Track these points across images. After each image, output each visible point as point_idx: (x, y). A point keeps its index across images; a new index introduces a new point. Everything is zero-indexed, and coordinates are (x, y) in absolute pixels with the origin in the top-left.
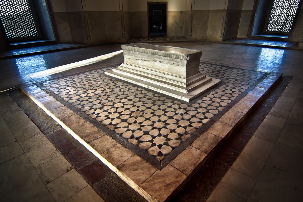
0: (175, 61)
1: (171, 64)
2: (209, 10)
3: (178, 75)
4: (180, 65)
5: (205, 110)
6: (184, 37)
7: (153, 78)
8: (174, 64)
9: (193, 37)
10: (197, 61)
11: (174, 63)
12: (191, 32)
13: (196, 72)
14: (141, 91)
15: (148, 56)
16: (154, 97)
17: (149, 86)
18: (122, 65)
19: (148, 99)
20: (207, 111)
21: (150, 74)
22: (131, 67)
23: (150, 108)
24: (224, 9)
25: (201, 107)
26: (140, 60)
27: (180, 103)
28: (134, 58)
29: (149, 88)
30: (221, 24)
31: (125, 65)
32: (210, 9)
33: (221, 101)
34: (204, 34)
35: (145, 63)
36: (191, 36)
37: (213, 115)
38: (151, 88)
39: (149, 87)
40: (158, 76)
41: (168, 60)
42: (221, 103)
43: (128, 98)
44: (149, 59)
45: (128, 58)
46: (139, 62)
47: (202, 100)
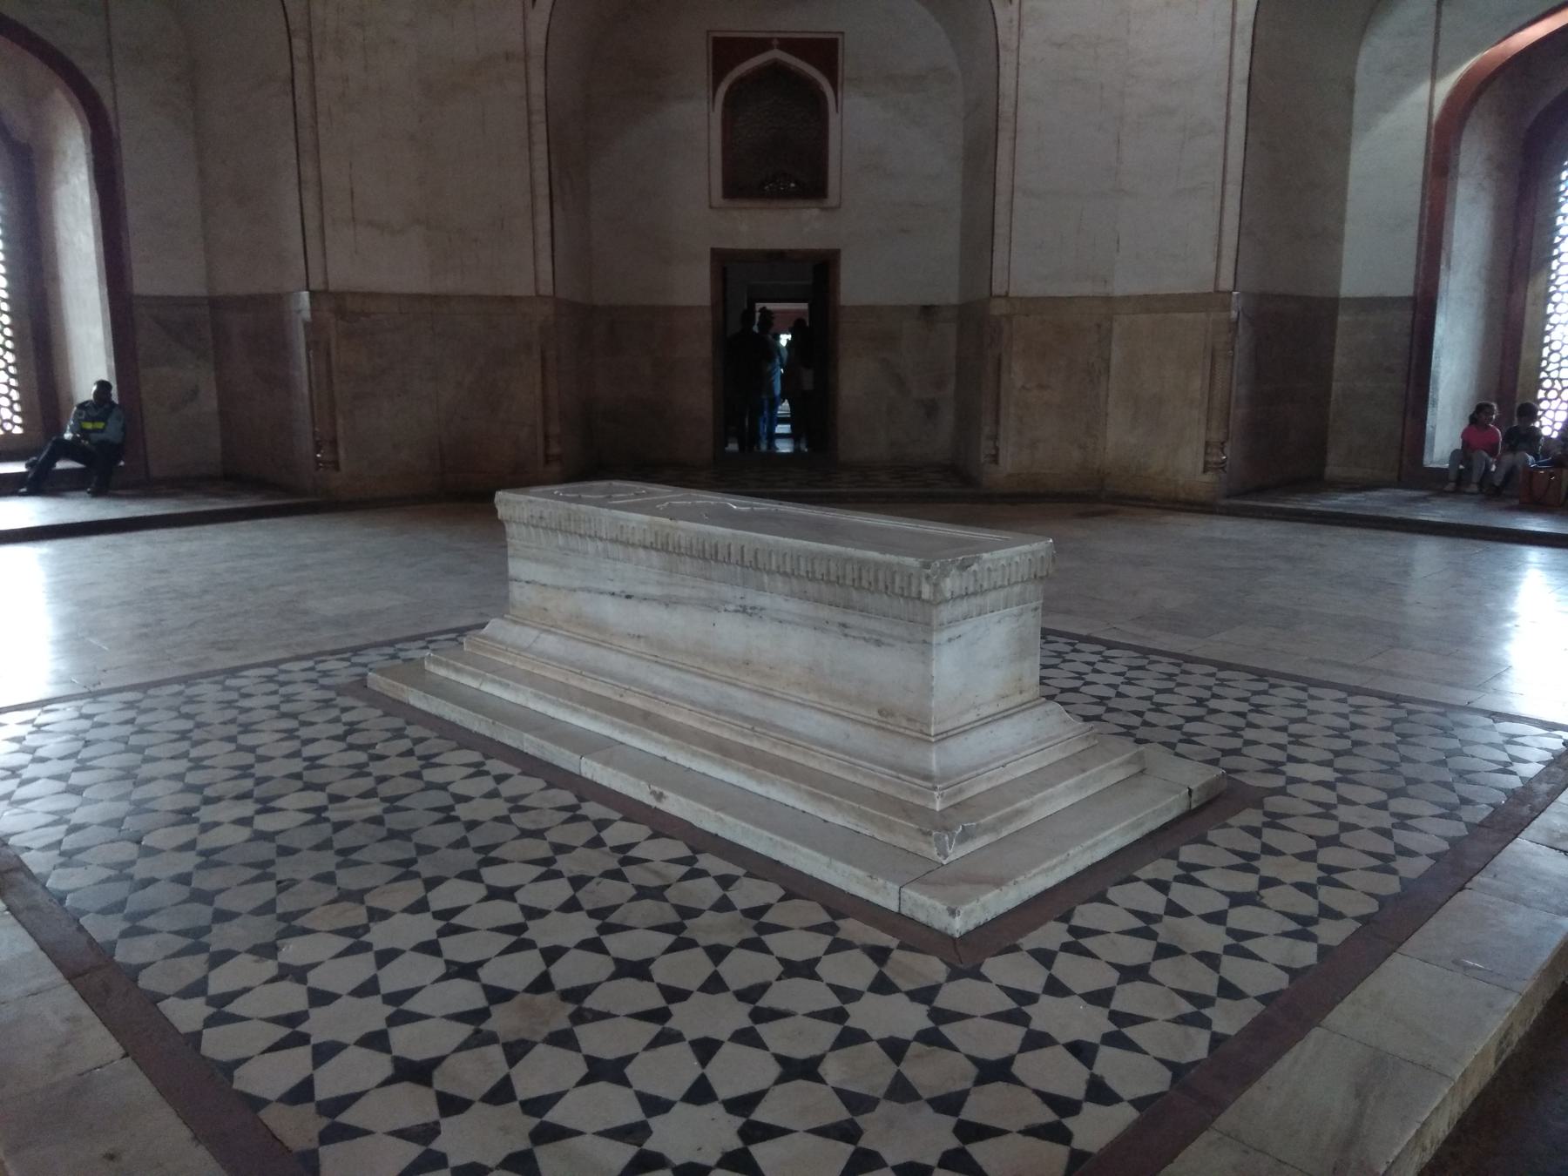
1: (820, 626)
2: (1108, 299)
3: (880, 712)
4: (891, 636)
5: (1090, 1024)
10: (1021, 614)
12: (995, 438)
13: (1018, 699)
14: (602, 824)
16: (684, 878)
19: (638, 887)
20: (1113, 1028)
21: (674, 696)
22: (551, 643)
23: (638, 970)
24: (1211, 289)
25: (1055, 988)
27: (886, 940)
28: (577, 584)
29: (663, 806)
30: (1197, 384)
32: (1118, 291)
33: (1229, 950)
35: (652, 618)
36: (995, 459)
37: (1164, 1069)
38: (675, 805)
39: (660, 797)
40: (733, 714)
41: (803, 596)
42: (1233, 969)
43: (493, 876)
46: (611, 611)
47: (1074, 931)
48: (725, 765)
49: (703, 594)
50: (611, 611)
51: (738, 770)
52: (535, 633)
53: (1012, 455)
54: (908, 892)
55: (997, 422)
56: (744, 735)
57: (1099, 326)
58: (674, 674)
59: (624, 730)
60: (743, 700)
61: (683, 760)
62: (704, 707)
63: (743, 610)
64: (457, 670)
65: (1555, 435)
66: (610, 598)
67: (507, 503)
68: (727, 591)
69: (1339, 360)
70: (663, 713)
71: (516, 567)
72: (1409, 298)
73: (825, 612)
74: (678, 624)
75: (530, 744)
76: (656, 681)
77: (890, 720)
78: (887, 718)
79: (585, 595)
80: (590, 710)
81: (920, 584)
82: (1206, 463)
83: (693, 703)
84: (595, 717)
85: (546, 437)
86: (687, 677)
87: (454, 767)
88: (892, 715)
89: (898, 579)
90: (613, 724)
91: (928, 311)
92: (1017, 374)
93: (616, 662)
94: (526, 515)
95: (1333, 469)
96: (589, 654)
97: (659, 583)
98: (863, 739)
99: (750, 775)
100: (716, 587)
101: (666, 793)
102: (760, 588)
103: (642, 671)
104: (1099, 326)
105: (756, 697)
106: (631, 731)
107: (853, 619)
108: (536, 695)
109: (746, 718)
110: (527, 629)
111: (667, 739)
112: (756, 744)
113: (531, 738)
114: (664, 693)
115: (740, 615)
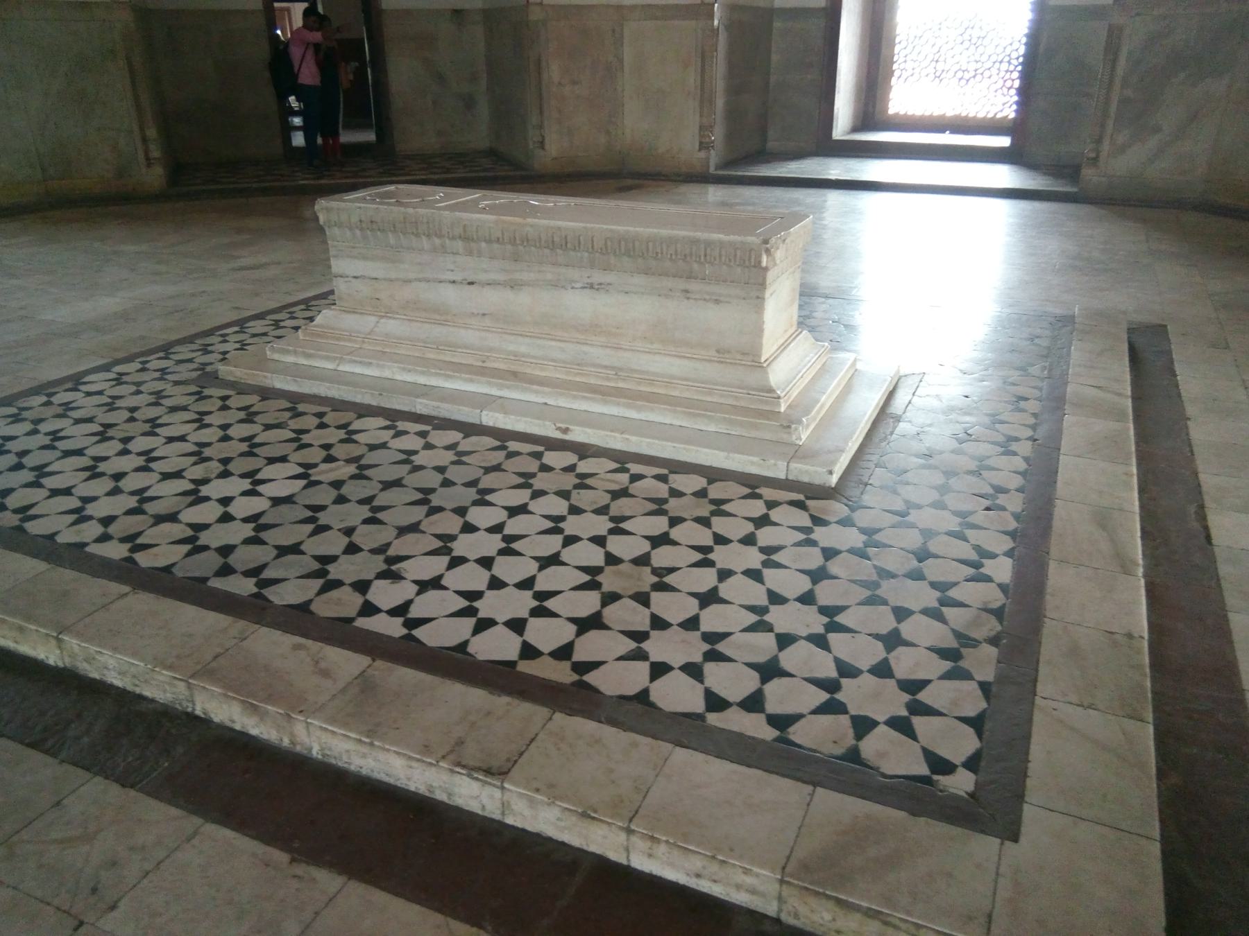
0: (690, 276)
2: (619, 8)
3: (718, 351)
6: (492, 153)
9: (554, 153)
11: (688, 287)
12: (541, 127)
15: (516, 258)
17: (563, 426)
18: (325, 317)
22: (391, 326)
28: (412, 276)
34: (608, 133)
35: (492, 298)
36: (542, 144)
38: (578, 435)
40: (594, 365)
41: (647, 272)
44: (517, 276)
45: (363, 277)
46: (450, 295)
48: (606, 403)
49: (549, 276)
51: (618, 404)
52: (373, 319)
53: (554, 145)
54: (793, 465)
55: (541, 113)
56: (608, 379)
57: (614, 31)
58: (527, 340)
59: (501, 387)
60: (597, 353)
61: (562, 402)
62: (564, 362)
63: (591, 286)
66: (451, 286)
67: (328, 210)
68: (573, 273)
69: (775, 58)
70: (528, 371)
71: (338, 266)
72: (824, 9)
73: (669, 283)
74: (522, 301)
75: (422, 406)
76: (511, 348)
78: (723, 354)
79: (423, 285)
81: (760, 256)
82: (701, 143)
83: (553, 360)
84: (471, 381)
85: (144, 140)
86: (539, 342)
89: (739, 253)
90: (489, 383)
91: (457, 13)
92: (554, 71)
93: (468, 336)
94: (354, 219)
95: (772, 145)
96: (437, 332)
98: (710, 371)
99: (628, 406)
100: (563, 270)
102: (607, 268)
103: (493, 340)
104: (614, 31)
105: (608, 351)
106: (508, 387)
107: (694, 286)
108: (404, 369)
109: (606, 367)
111: (546, 389)
112: (621, 385)
115: (587, 291)
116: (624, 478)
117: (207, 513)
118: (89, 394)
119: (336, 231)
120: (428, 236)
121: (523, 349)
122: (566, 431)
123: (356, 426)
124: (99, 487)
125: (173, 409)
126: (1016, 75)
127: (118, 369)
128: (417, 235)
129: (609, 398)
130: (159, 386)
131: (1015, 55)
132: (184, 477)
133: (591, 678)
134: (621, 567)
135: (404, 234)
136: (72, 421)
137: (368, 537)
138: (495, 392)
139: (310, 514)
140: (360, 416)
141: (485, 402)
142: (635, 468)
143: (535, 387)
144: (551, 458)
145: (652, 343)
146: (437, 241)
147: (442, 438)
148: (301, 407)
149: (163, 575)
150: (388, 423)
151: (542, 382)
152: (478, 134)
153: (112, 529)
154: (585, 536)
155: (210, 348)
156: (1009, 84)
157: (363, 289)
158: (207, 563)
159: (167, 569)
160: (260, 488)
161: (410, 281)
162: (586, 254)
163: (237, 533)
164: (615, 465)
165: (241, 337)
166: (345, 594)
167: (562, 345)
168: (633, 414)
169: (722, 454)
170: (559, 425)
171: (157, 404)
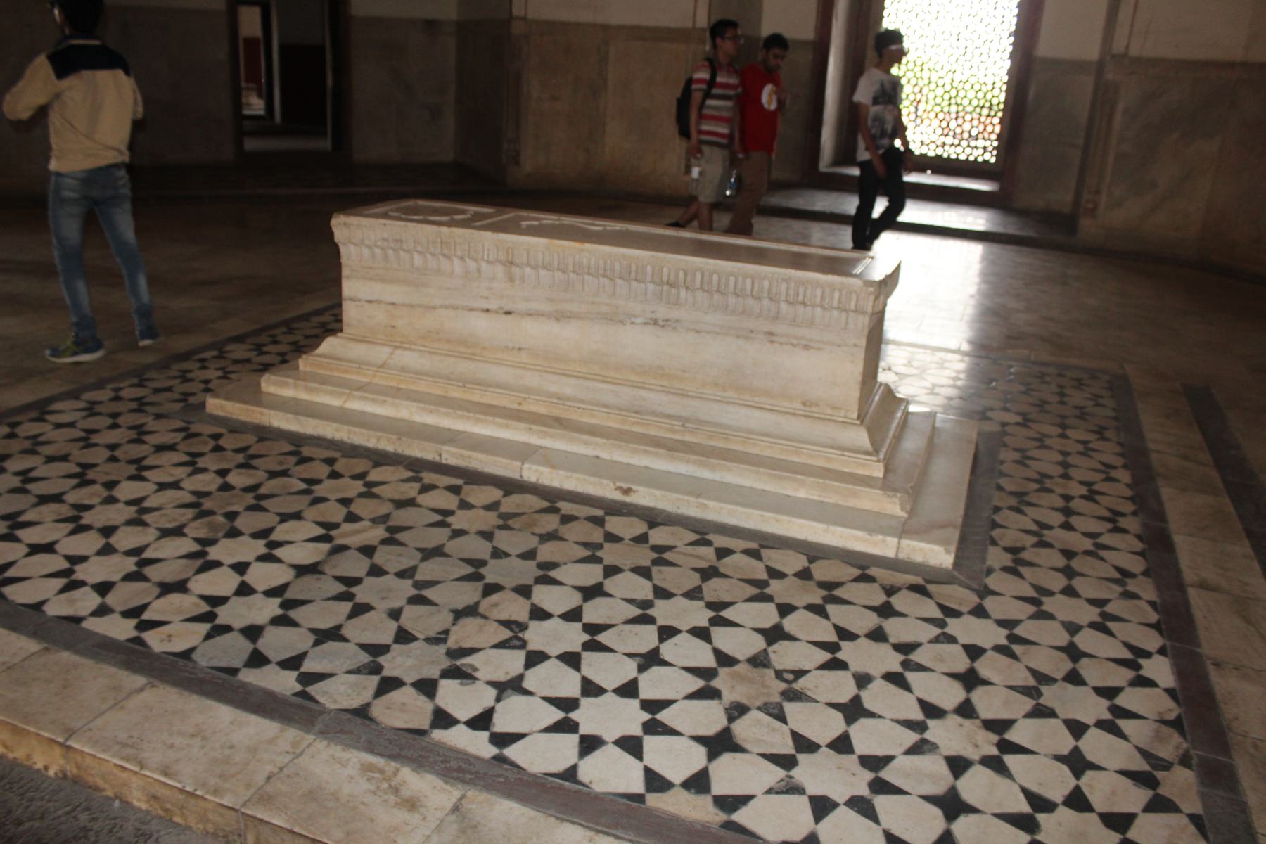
2: (605, 27)
3: (804, 404)
7: (621, 432)
8: (773, 338)
17: (625, 486)
18: (329, 345)
21: (582, 402)
22: (409, 358)
26: (488, 311)
28: (437, 302)
29: (627, 499)
31: (352, 344)
35: (535, 332)
36: (516, 161)
38: (643, 497)
40: (654, 413)
45: (379, 302)
46: (480, 325)
49: (604, 309)
50: (480, 325)
51: (688, 462)
56: (673, 431)
64: (311, 390)
65: (993, 160)
66: (484, 315)
75: (451, 456)
76: (554, 389)
77: (814, 409)
80: (498, 420)
83: (606, 406)
84: (507, 426)
87: (393, 482)
88: (817, 405)
91: (431, 26)
97: (551, 300)
101: (634, 487)
102: (677, 303)
103: (532, 380)
106: (552, 436)
109: (669, 416)
110: (378, 348)
111: (599, 440)
113: (454, 450)
114: (568, 399)
115: (650, 328)
116: (708, 552)
117: (221, 582)
118: (59, 426)
119: (352, 248)
120: (462, 258)
121: (568, 391)
122: (627, 491)
123: (374, 476)
124: (87, 543)
125: (160, 448)
126: (996, 120)
127: (88, 396)
128: (448, 257)
129: (676, 454)
130: (138, 419)
131: (995, 101)
132: (184, 535)
133: (742, 816)
134: (737, 668)
135: (433, 255)
136: (43, 460)
137: (418, 620)
138: (535, 440)
139: (342, 588)
140: (377, 464)
141: (525, 453)
142: (720, 541)
143: (586, 437)
144: (615, 524)
145: (725, 391)
146: (472, 265)
147: (482, 495)
148: (306, 451)
149: (181, 662)
150: (410, 474)
151: (594, 431)
152: (442, 145)
153: (111, 599)
154: (685, 627)
155: (189, 375)
156: (990, 129)
157: (379, 316)
158: (233, 649)
159: (187, 655)
160: (278, 552)
161: (434, 308)
162: (651, 287)
163: (263, 610)
164: (694, 537)
165: (222, 363)
166: (407, 695)
167: (615, 388)
168: (706, 474)
169: (821, 526)
170: (619, 484)
171: (139, 441)
